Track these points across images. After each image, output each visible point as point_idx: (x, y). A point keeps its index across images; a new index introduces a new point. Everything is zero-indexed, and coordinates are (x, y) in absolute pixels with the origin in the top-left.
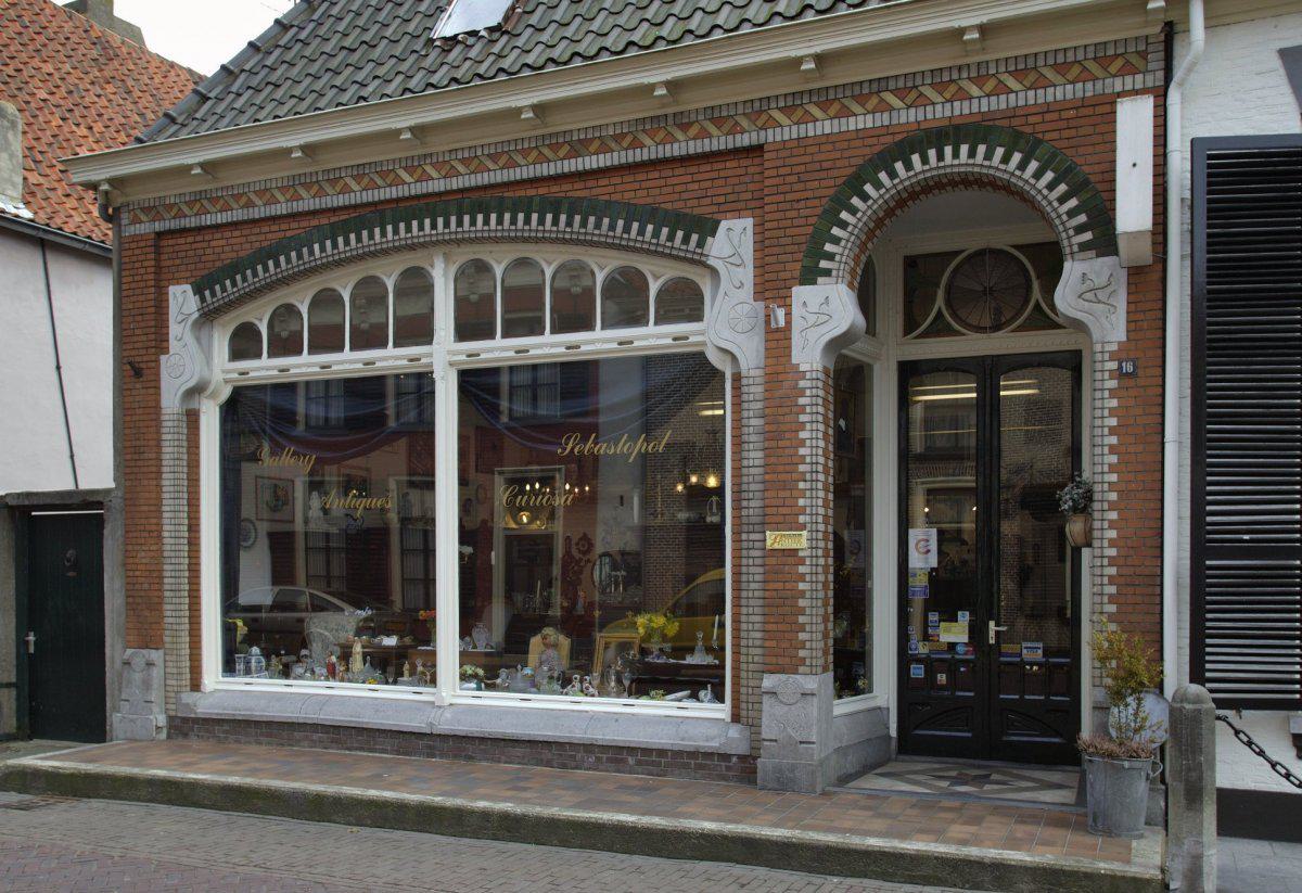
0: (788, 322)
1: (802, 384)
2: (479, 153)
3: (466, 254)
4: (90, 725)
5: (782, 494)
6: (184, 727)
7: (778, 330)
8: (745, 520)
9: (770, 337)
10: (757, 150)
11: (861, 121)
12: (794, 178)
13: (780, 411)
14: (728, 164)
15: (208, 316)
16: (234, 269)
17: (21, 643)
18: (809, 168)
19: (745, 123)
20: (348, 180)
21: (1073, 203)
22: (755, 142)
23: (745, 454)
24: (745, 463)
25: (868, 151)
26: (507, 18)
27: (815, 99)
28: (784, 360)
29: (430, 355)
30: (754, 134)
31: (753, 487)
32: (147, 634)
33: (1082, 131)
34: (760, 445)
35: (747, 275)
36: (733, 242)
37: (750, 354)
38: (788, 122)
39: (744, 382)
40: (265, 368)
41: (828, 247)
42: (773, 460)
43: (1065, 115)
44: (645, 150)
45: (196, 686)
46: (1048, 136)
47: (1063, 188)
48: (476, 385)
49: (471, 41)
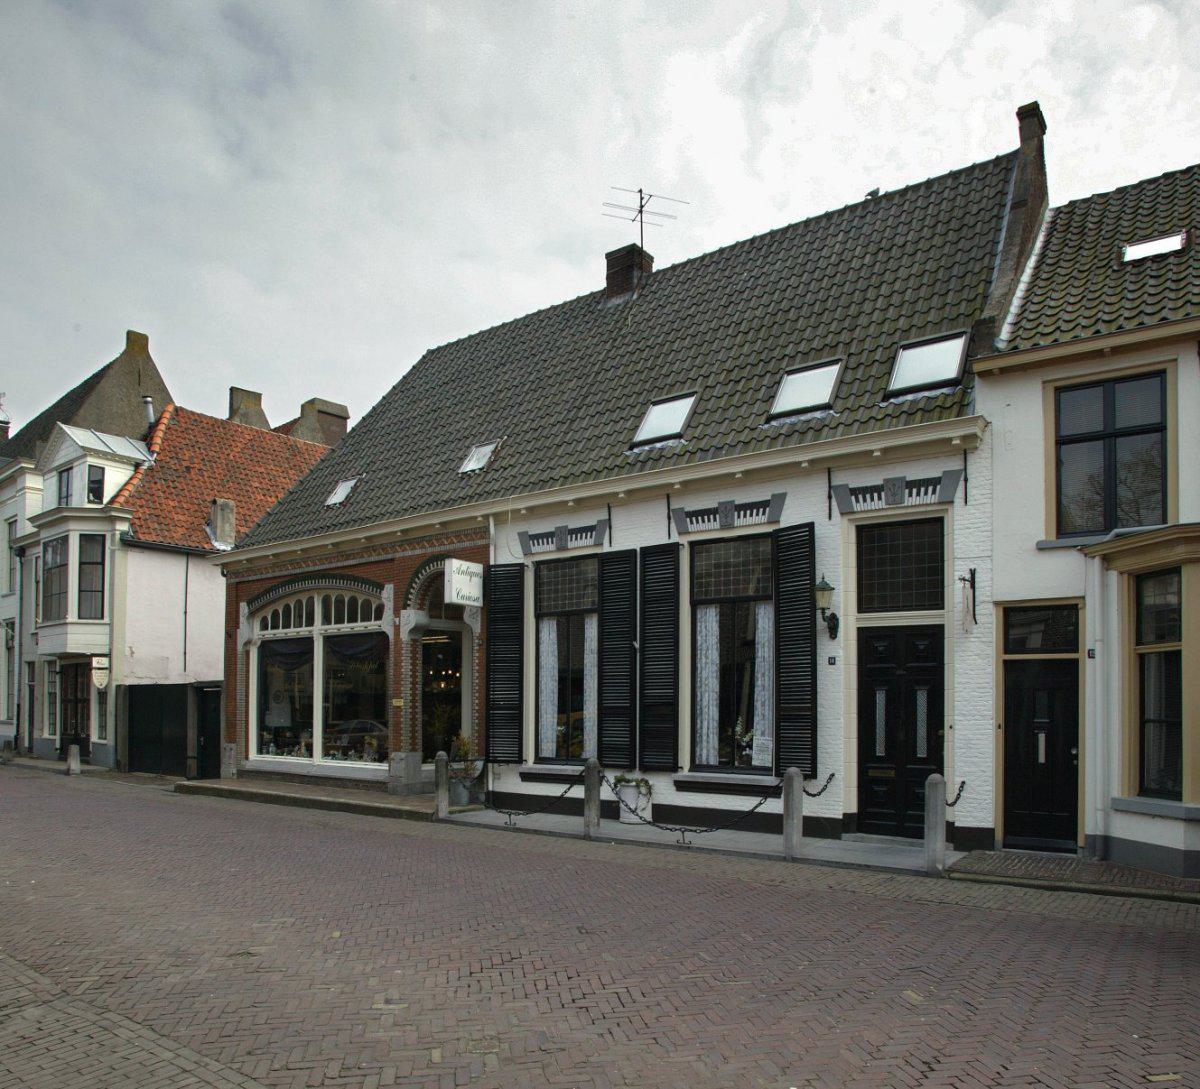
3: (324, 593)
4: (216, 775)
6: (244, 774)
10: (392, 560)
11: (418, 552)
15: (252, 615)
16: (258, 597)
17: (199, 741)
32: (232, 739)
40: (270, 634)
45: (247, 758)
48: (329, 640)
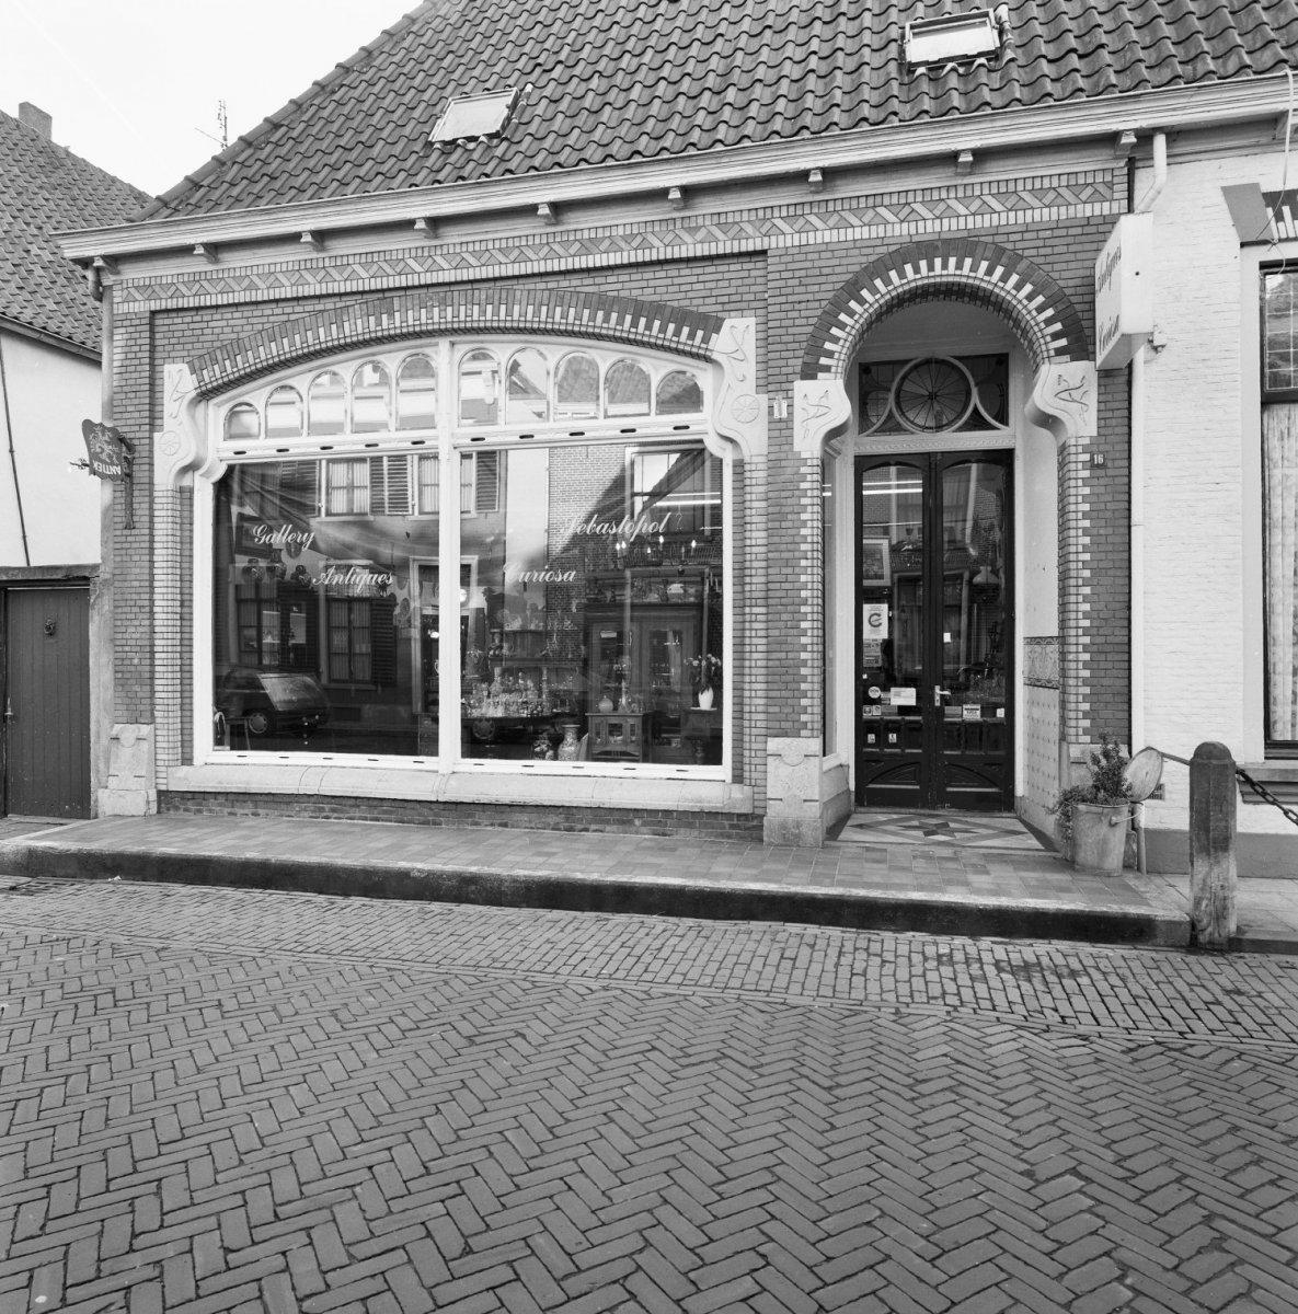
0: (790, 414)
1: (803, 470)
2: (490, 246)
5: (784, 571)
7: (780, 420)
8: (748, 595)
9: (773, 426)
10: (764, 252)
12: (796, 282)
13: (784, 494)
14: (732, 267)
18: (810, 272)
19: (749, 229)
20: (357, 268)
21: (1050, 312)
22: (759, 248)
23: (748, 534)
24: (748, 542)
25: (864, 259)
26: (504, 127)
27: (815, 210)
28: (786, 448)
29: (436, 438)
30: (758, 241)
31: (755, 564)
33: (1056, 250)
34: (763, 526)
35: (750, 369)
36: (738, 337)
37: (755, 443)
38: (790, 231)
39: (747, 467)
41: (828, 346)
42: (776, 539)
43: (1041, 234)
44: (654, 251)
46: (1027, 253)
47: (1040, 299)
49: (471, 146)
